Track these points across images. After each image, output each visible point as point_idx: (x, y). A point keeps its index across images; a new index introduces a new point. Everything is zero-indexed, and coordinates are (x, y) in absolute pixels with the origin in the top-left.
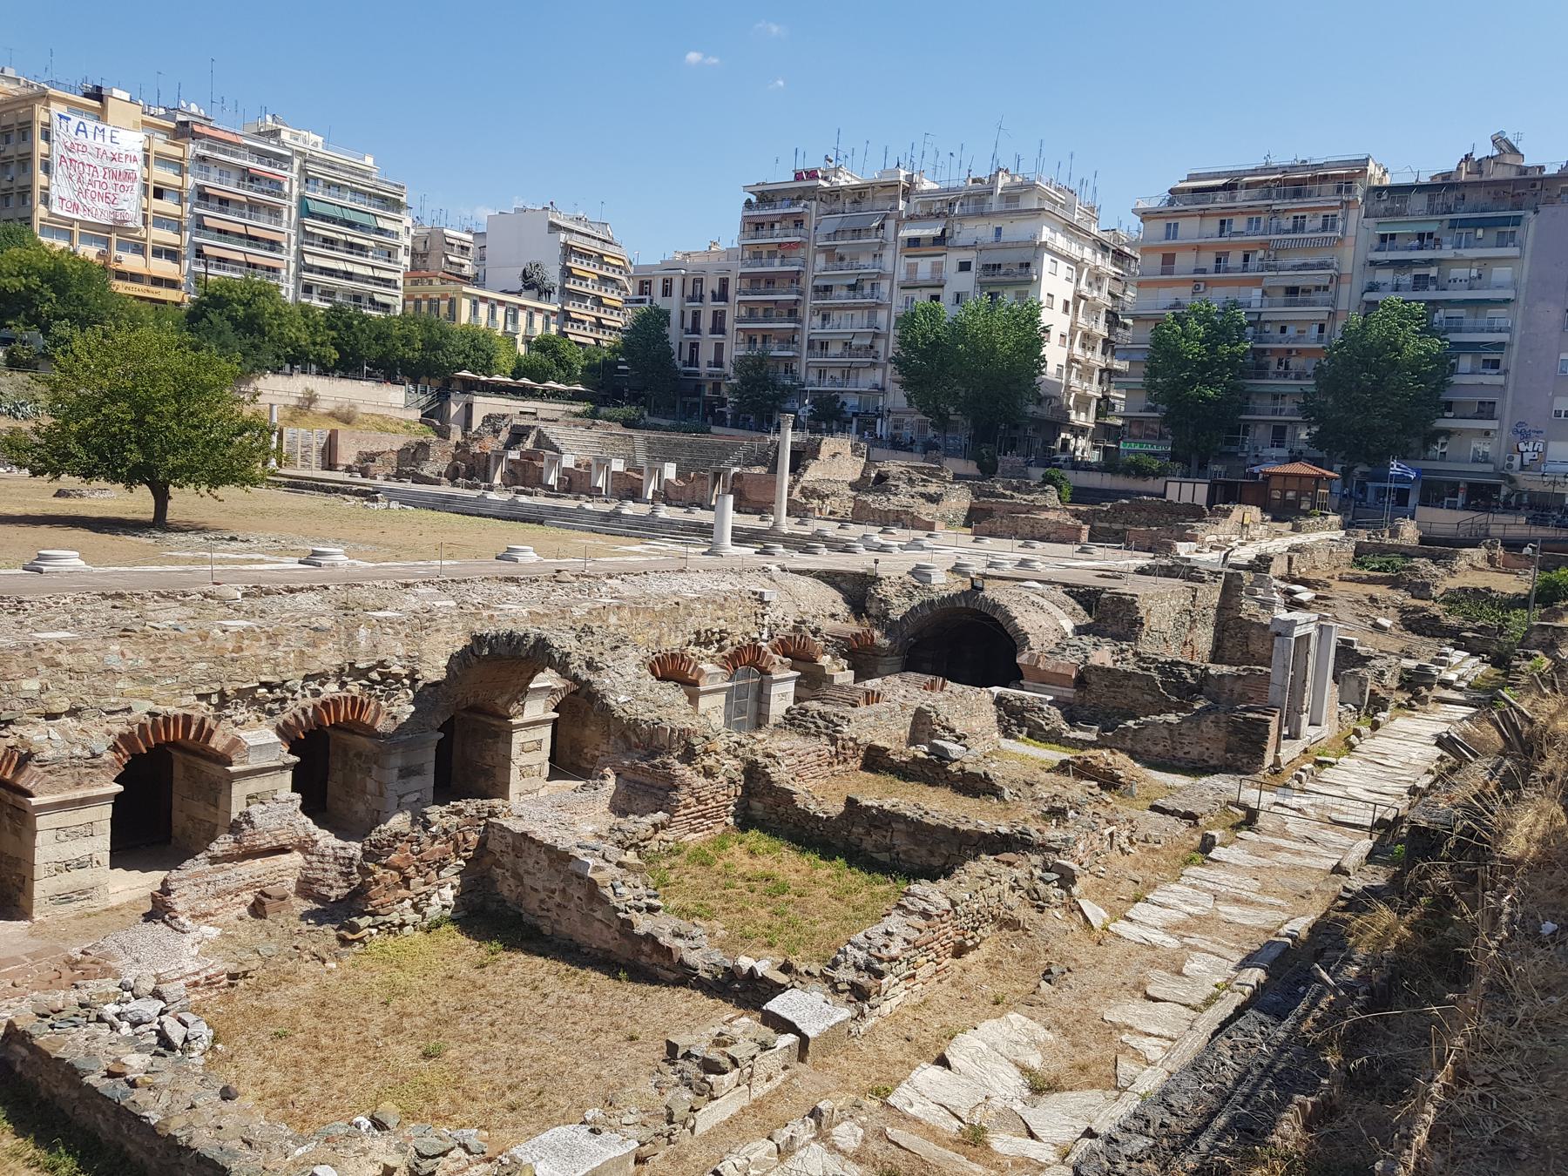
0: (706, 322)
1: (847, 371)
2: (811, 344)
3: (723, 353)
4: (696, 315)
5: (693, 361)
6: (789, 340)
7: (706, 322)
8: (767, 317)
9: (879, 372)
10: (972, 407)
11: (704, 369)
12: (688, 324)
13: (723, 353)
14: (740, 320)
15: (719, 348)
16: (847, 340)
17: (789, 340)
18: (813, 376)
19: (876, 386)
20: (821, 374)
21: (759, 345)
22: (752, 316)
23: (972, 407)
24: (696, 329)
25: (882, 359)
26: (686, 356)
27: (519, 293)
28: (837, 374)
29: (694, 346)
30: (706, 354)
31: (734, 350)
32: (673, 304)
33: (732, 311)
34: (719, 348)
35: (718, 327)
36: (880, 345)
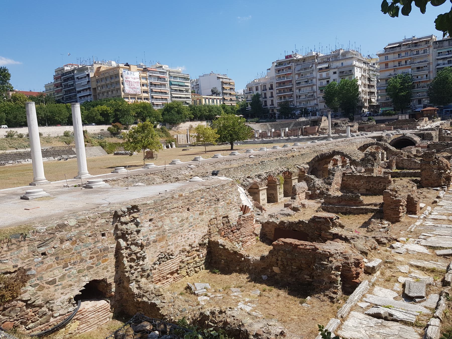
0: (268, 95)
1: (307, 102)
2: (297, 97)
3: (274, 101)
4: (265, 94)
5: (266, 105)
6: (291, 96)
7: (268, 95)
8: (284, 92)
9: (316, 101)
10: (344, 103)
11: (269, 106)
12: (263, 96)
13: (274, 101)
14: (277, 94)
15: (272, 101)
16: (310, 93)
17: (291, 96)
18: (298, 104)
19: (315, 104)
20: (300, 103)
21: (283, 99)
22: (280, 92)
23: (344, 103)
24: (266, 97)
25: (316, 98)
26: (264, 104)
27: (212, 95)
28: (305, 103)
29: (266, 101)
30: (269, 103)
31: (276, 101)
32: (259, 92)
33: (275, 92)
34: (272, 101)
35: (272, 96)
36: (315, 94)
